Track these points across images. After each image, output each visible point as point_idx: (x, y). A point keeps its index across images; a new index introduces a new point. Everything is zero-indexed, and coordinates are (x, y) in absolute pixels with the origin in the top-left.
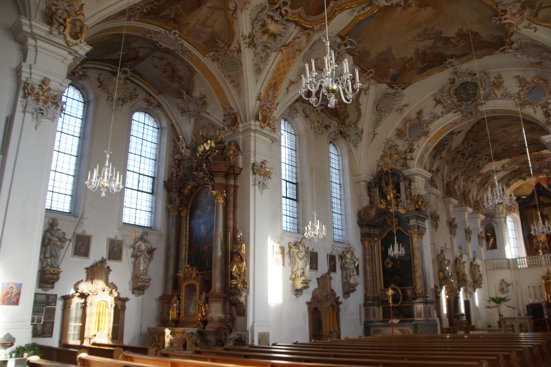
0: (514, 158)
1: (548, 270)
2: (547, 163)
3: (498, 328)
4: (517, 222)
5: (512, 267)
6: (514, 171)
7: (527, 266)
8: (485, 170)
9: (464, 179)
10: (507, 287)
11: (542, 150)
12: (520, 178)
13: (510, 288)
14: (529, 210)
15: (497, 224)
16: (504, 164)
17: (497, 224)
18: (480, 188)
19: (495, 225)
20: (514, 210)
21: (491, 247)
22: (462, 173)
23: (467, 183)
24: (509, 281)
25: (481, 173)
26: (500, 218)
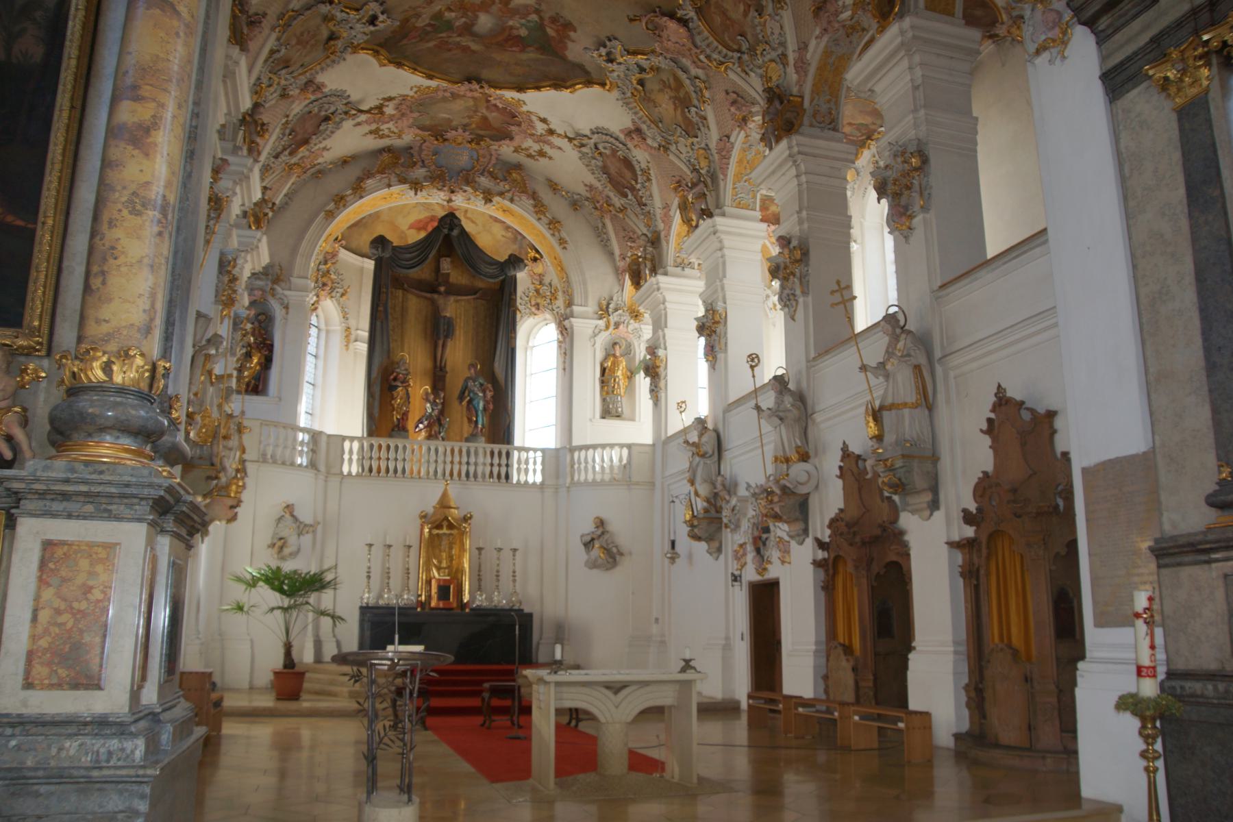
0: (433, 83)
1: (445, 495)
2: (494, 161)
3: (267, 701)
4: (328, 332)
5: (322, 468)
6: (389, 150)
7: (355, 469)
8: (333, 79)
9: (272, 52)
10: (299, 535)
11: (538, 88)
12: (403, 181)
13: (307, 539)
14: (400, 293)
15: (287, 307)
16: (390, 99)
17: (287, 307)
18: (285, 149)
19: (278, 312)
20: (332, 289)
21: (248, 385)
22: (281, 16)
23: (270, 86)
24: (305, 516)
25: (320, 78)
26: (305, 289)
